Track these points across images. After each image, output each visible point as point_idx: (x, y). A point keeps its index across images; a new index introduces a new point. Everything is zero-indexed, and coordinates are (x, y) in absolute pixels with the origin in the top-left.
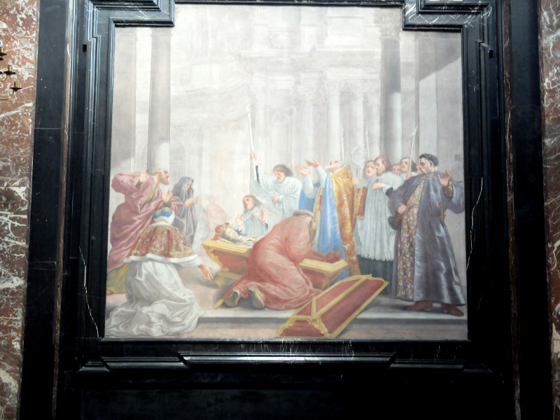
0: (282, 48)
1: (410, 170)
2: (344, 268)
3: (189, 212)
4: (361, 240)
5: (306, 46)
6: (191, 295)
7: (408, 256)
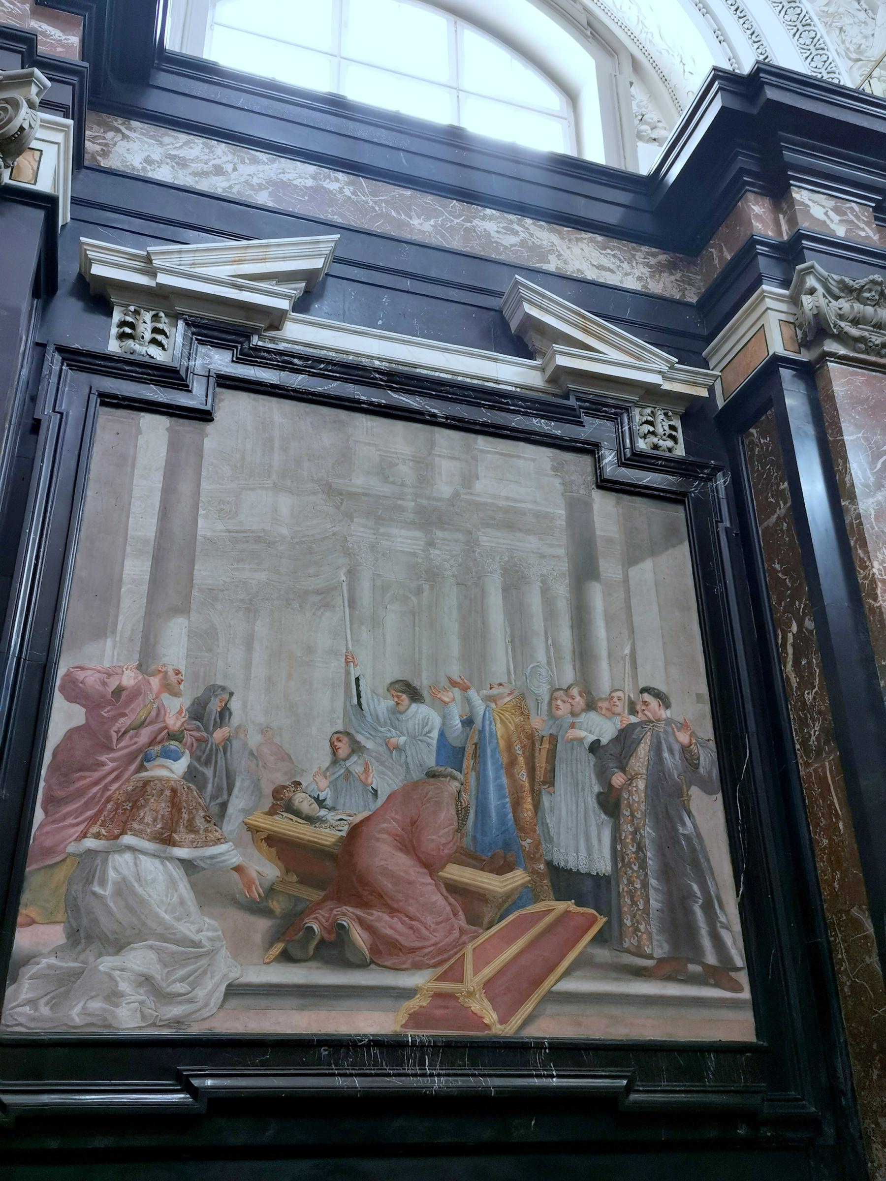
0: (403, 485)
1: (626, 711)
2: (524, 886)
3: (221, 755)
4: (552, 831)
5: (444, 488)
6: (216, 930)
7: (636, 868)
